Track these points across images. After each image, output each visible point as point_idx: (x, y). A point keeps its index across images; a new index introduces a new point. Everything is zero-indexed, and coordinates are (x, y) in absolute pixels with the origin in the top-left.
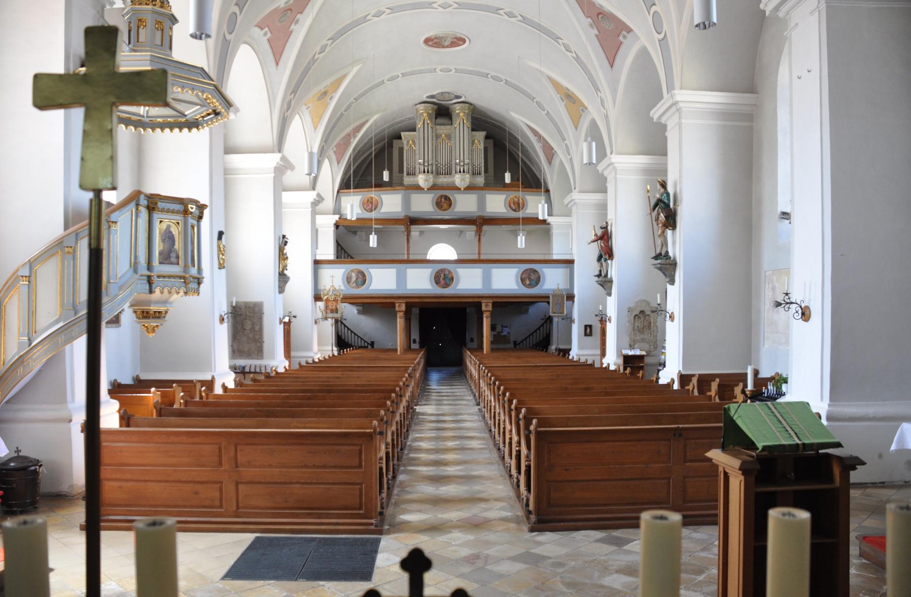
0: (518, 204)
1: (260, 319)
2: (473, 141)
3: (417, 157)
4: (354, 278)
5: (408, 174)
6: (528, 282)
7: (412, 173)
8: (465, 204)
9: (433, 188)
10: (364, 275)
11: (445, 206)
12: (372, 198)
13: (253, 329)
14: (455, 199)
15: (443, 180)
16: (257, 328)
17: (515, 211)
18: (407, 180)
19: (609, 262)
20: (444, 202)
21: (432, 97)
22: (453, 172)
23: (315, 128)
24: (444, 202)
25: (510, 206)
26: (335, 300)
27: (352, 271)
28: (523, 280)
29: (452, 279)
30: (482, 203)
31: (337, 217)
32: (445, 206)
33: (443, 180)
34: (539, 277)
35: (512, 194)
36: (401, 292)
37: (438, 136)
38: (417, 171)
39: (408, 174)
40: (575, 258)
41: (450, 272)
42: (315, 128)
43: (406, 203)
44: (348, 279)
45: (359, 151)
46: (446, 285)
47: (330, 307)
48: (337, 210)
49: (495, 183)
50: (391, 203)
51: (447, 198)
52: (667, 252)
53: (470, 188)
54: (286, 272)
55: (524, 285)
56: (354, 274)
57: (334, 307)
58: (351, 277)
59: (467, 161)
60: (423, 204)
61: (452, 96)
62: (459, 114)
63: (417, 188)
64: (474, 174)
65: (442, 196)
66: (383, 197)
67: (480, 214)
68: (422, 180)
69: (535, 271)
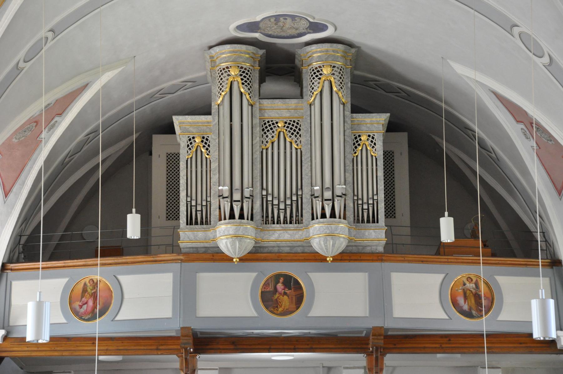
0: (477, 297)
2: (357, 139)
3: (215, 178)
5: (190, 222)
11: (285, 302)
12: (95, 284)
15: (281, 236)
17: (468, 314)
18: (189, 237)
20: (282, 293)
30: (380, 296)
32: (285, 302)
33: (281, 236)
37: (267, 126)
38: (215, 213)
39: (190, 222)
43: (185, 295)
45: (63, 164)
49: (416, 244)
53: (350, 256)
59: (339, 189)
60: (229, 299)
61: (303, 25)
62: (317, 73)
63: (214, 257)
64: (358, 220)
65: (277, 277)
67: (377, 323)
68: (225, 236)
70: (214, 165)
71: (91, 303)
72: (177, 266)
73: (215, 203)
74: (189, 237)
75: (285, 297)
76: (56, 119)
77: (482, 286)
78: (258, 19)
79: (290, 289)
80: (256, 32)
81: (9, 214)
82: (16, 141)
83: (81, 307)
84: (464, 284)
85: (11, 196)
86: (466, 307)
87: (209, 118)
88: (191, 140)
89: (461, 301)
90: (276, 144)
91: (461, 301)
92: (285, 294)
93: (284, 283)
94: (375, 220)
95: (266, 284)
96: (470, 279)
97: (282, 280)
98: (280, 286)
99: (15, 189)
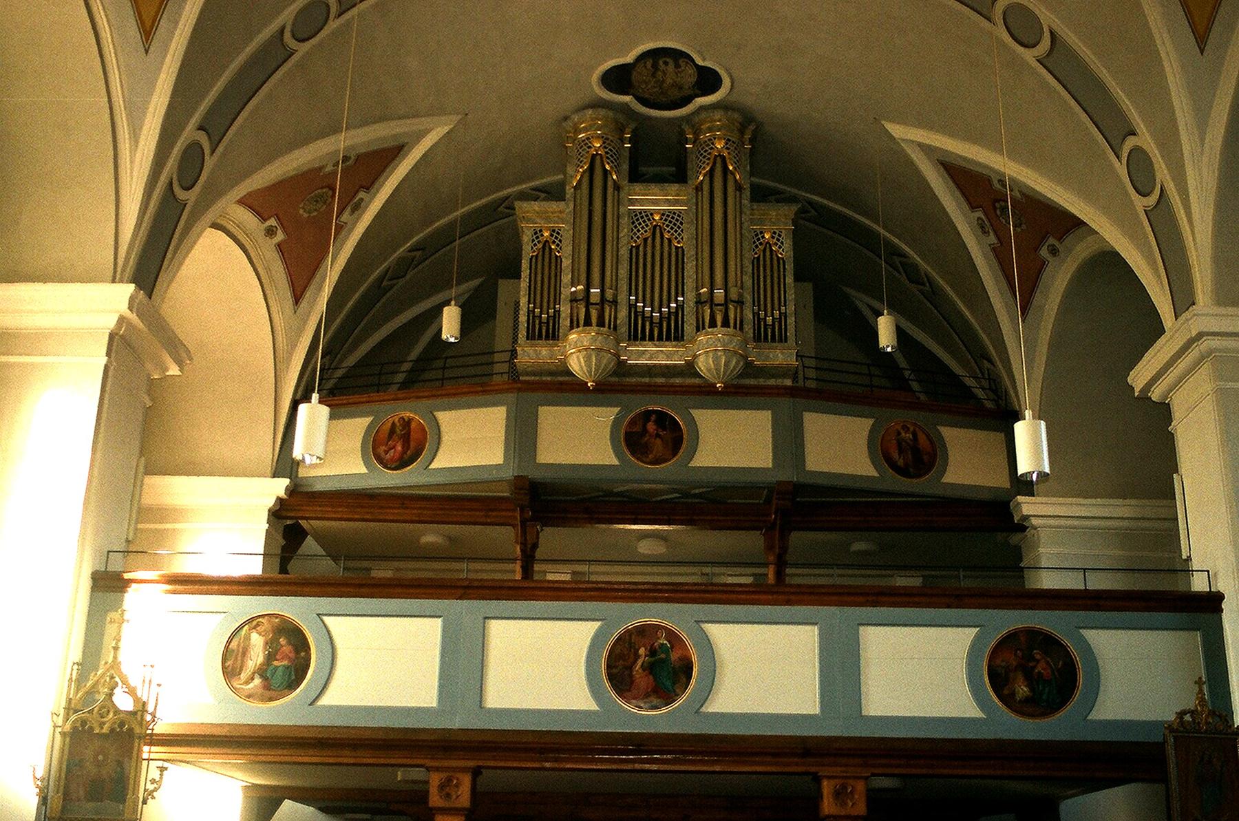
0: (915, 449)
3: (566, 278)
4: (257, 656)
5: (530, 336)
6: (1022, 690)
7: (548, 331)
8: (733, 443)
9: (614, 384)
10: (300, 643)
12: (407, 423)
14: (692, 423)
17: (903, 471)
18: (532, 355)
20: (653, 432)
21: (618, 79)
22: (689, 328)
23: (147, 32)
27: (252, 622)
28: (999, 679)
29: (686, 669)
31: (280, 486)
38: (565, 322)
39: (530, 336)
40: (1222, 586)
42: (147, 32)
43: (522, 435)
45: (378, 289)
48: (285, 464)
50: (470, 442)
55: (1007, 699)
56: (257, 641)
58: (245, 652)
60: (579, 440)
63: (563, 387)
65: (647, 415)
66: (442, 416)
67: (787, 475)
68: (578, 352)
69: (1049, 643)
70: (566, 263)
71: (399, 448)
72: (511, 397)
73: (565, 309)
74: (532, 355)
75: (658, 441)
76: (361, 195)
77: (922, 438)
78: (629, 58)
79: (664, 429)
80: (627, 94)
81: (300, 331)
82: (306, 215)
83: (386, 452)
84: (899, 433)
85: (304, 304)
86: (901, 463)
87: (562, 205)
88: (538, 233)
89: (895, 455)
90: (649, 241)
92: (658, 436)
93: (656, 422)
94: (783, 339)
95: (633, 422)
97: (653, 417)
98: (651, 426)
99: (308, 294)
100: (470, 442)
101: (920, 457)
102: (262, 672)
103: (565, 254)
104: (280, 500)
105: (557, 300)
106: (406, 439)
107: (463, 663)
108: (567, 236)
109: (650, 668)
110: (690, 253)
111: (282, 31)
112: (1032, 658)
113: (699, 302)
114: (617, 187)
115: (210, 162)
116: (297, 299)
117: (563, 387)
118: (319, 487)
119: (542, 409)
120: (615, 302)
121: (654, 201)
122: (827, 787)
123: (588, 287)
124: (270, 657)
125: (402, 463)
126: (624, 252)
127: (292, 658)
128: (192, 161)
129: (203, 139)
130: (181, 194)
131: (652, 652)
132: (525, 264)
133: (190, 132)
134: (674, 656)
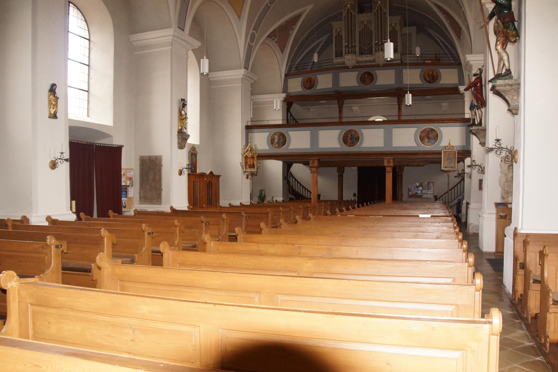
0: (433, 76)
1: (160, 170)
3: (344, 41)
4: (276, 140)
12: (310, 78)
13: (154, 179)
16: (157, 178)
17: (429, 82)
18: (337, 61)
19: (483, 110)
20: (367, 77)
22: (374, 52)
23: (239, 17)
24: (367, 77)
25: (425, 79)
26: (252, 157)
27: (275, 134)
28: (422, 139)
29: (358, 139)
31: (284, 95)
34: (437, 136)
35: (427, 68)
36: (315, 150)
41: (356, 132)
43: (336, 80)
44: (272, 141)
46: (353, 144)
47: (249, 163)
51: (369, 74)
52: (509, 72)
54: (185, 130)
56: (276, 137)
57: (252, 163)
60: (349, 80)
65: (365, 73)
67: (398, 86)
69: (432, 130)
70: (344, 37)
74: (337, 61)
77: (434, 73)
85: (284, 53)
86: (428, 80)
89: (427, 78)
91: (427, 78)
95: (362, 75)
96: (430, 71)
98: (366, 76)
100: (324, 82)
101: (434, 78)
102: (278, 143)
103: (343, 34)
104: (285, 98)
105: (342, 47)
106: (311, 82)
107: (314, 139)
108: (343, 29)
109: (351, 139)
110: (373, 32)
111: (267, 4)
112: (429, 134)
113: (376, 45)
114: (354, 16)
115: (256, 35)
116: (282, 52)
117: (346, 68)
118: (292, 95)
119: (341, 73)
120: (355, 46)
121: (364, 17)
122: (385, 161)
123: (348, 44)
124: (279, 140)
125: (310, 88)
126: (357, 33)
127: (283, 140)
128: (253, 36)
129: (254, 31)
130: (251, 44)
131: (351, 135)
132: (334, 38)
133: (251, 31)
134: (356, 136)
